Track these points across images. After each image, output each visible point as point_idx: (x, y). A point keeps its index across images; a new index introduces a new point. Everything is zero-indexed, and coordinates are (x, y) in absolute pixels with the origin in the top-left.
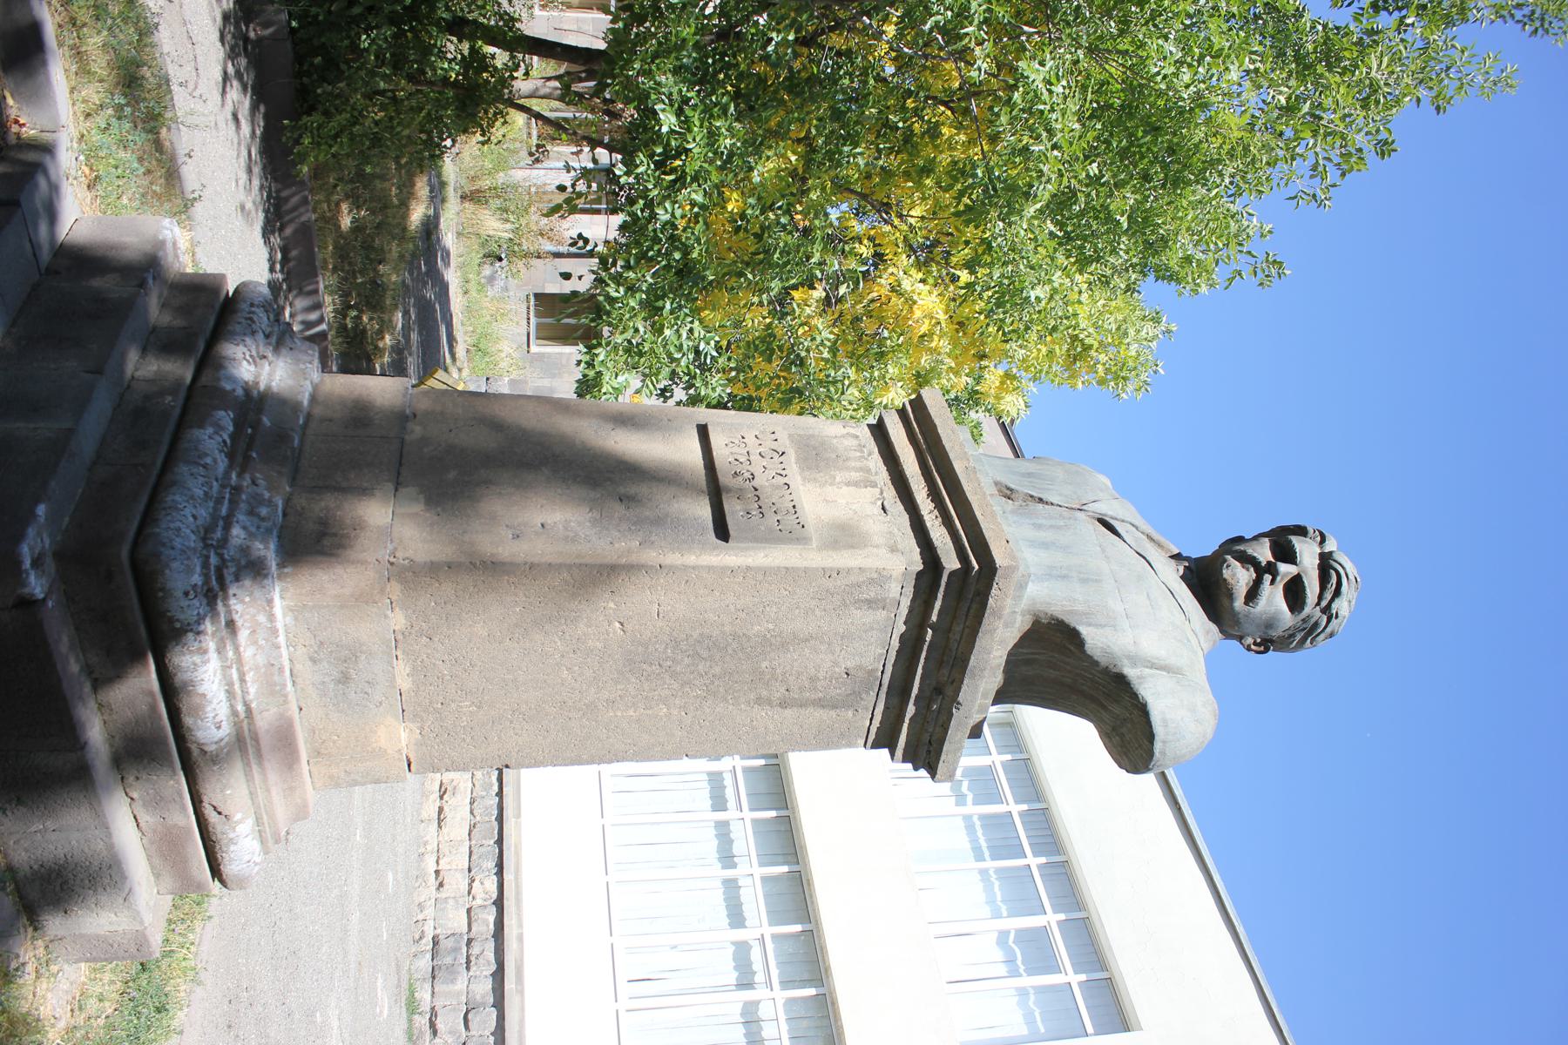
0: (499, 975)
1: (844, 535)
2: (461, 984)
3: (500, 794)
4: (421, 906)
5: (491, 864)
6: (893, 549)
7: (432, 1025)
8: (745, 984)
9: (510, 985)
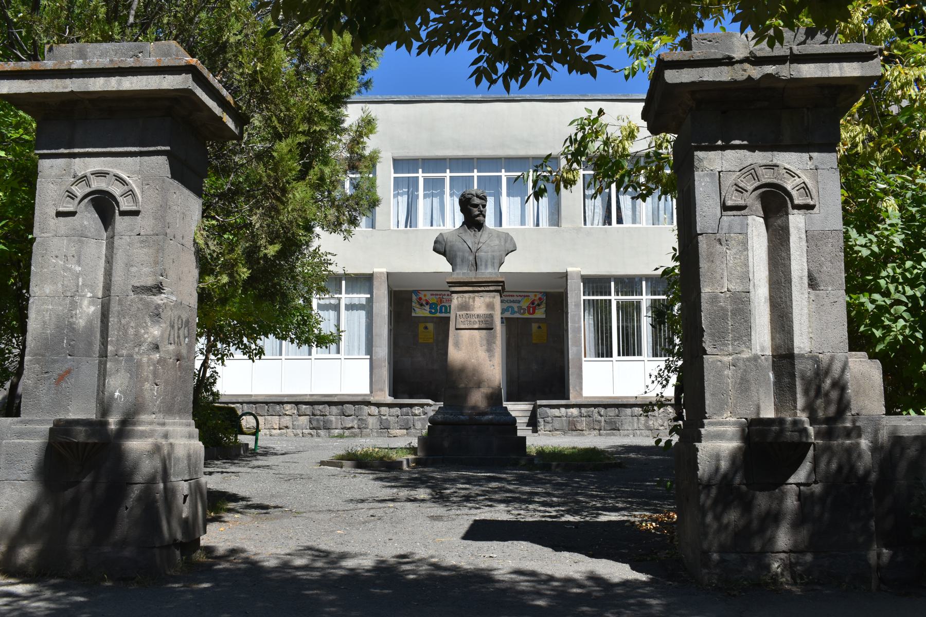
0: (330, 404)
1: (490, 306)
2: (333, 418)
5: (278, 407)
7: (349, 428)
8: (336, 308)
9: (336, 399)
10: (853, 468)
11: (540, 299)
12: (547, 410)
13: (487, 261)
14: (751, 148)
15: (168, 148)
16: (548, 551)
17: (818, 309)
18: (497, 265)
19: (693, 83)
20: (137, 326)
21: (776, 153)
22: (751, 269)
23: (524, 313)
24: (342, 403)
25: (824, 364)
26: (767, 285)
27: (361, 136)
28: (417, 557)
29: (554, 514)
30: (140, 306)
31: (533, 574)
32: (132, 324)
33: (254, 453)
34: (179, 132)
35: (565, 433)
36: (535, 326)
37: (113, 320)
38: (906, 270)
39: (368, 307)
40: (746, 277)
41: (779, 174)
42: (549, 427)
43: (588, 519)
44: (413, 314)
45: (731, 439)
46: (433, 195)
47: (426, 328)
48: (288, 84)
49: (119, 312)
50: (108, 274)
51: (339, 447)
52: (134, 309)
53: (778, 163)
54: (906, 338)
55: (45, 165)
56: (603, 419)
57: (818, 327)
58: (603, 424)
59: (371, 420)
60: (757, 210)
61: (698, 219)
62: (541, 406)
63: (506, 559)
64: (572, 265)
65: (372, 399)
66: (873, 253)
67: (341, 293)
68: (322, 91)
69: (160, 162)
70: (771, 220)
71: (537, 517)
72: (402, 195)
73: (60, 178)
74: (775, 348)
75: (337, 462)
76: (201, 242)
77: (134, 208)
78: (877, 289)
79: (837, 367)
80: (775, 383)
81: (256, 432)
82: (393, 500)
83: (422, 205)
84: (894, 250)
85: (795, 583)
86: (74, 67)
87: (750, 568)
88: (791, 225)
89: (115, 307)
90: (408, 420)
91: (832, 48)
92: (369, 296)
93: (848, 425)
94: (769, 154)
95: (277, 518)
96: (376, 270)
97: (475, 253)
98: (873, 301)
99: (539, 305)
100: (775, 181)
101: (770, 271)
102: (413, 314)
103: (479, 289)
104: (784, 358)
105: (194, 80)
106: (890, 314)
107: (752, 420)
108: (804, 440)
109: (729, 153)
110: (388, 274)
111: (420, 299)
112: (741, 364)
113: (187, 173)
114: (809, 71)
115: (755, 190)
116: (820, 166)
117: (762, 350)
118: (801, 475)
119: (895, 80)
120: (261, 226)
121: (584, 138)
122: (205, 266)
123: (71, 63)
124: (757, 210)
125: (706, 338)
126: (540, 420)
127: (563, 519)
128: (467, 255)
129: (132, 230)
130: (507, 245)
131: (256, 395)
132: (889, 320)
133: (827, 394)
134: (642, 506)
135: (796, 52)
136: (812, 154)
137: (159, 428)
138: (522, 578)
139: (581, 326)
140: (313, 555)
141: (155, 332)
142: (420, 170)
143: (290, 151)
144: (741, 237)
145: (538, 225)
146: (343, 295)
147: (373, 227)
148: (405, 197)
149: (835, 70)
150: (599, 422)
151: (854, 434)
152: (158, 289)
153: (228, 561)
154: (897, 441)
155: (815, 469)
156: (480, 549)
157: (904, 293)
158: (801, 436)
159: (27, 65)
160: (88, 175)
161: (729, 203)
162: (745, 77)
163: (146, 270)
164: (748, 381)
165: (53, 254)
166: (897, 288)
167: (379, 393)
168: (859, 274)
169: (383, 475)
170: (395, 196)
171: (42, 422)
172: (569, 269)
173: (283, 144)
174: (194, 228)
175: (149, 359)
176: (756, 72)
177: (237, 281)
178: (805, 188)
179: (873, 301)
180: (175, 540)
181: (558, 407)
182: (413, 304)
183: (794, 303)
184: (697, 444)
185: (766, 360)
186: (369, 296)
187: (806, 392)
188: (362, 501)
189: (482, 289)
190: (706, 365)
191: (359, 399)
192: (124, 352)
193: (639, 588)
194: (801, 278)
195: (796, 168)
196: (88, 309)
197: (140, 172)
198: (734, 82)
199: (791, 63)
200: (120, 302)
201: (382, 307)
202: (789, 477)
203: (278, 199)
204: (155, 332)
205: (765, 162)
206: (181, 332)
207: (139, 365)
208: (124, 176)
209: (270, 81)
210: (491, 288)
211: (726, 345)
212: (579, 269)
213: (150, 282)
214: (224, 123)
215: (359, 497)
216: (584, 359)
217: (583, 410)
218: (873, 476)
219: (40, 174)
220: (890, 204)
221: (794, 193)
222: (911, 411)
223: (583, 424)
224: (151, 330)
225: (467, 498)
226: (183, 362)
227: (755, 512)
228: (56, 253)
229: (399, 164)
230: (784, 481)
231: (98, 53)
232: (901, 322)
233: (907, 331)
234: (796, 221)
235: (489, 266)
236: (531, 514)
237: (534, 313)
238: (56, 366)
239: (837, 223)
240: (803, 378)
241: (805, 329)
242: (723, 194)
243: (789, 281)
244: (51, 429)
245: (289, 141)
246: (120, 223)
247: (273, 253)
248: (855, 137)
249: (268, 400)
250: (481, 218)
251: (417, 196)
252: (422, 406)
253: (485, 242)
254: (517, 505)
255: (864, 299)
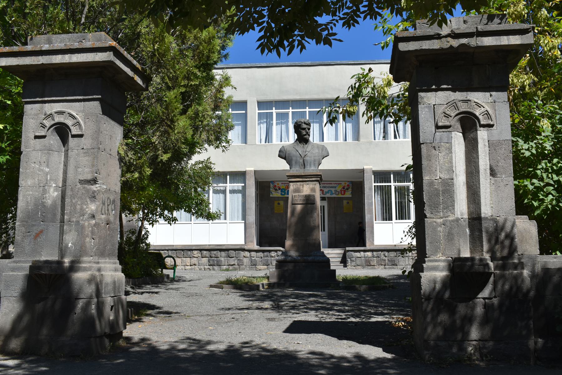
0: (221, 250)
1: (313, 190)
2: (222, 259)
3: (168, 250)
4: (200, 269)
5: (189, 252)
6: (315, 185)
7: (232, 265)
8: (224, 192)
9: (224, 248)
10: (519, 288)
11: (348, 185)
12: (353, 253)
13: (311, 162)
14: (454, 90)
15: (100, 97)
16: (334, 340)
17: (496, 188)
18: (317, 165)
19: (416, 50)
20: (82, 204)
21: (469, 93)
22: (454, 164)
23: (339, 194)
24: (228, 250)
25: (500, 224)
26: (465, 175)
27: (221, 87)
28: (254, 343)
29: (344, 317)
30: (84, 192)
31: (321, 354)
32: (79, 203)
33: (173, 280)
34: (107, 87)
35: (363, 267)
36: (345, 202)
37: (67, 200)
38: (553, 165)
39: (243, 192)
40: (451, 170)
41: (471, 106)
42: (353, 264)
43: (364, 320)
44: (271, 196)
45: (442, 271)
46: (282, 123)
47: (279, 204)
48: (173, 58)
49: (71, 195)
50: (65, 172)
51: (222, 276)
52: (80, 193)
53: (471, 99)
54: (553, 206)
55: (28, 107)
56: (387, 259)
57: (497, 200)
58: (387, 261)
59: (246, 261)
60: (458, 128)
61: (421, 134)
62: (349, 251)
63: (306, 345)
64: (367, 165)
65: (246, 247)
66: (532, 153)
67: (226, 183)
68: (195, 60)
69: (95, 105)
70: (467, 134)
71: (333, 319)
72: (263, 123)
73: (37, 116)
74: (470, 213)
75: (219, 286)
76: (122, 153)
77: (80, 133)
78: (535, 176)
79: (508, 225)
80: (470, 236)
81: (174, 267)
82: (247, 309)
83: (275, 129)
84: (546, 152)
85: (482, 360)
86: (44, 49)
87: (455, 350)
88: (479, 137)
89: (69, 193)
90: (268, 260)
91: (503, 27)
92: (243, 185)
93: (516, 261)
94: (465, 93)
95: (176, 319)
96: (247, 169)
97: (303, 158)
98: (533, 184)
99: (347, 189)
100: (469, 110)
101: (467, 166)
102: (271, 196)
103: (306, 180)
104: (475, 220)
105: (114, 55)
106: (544, 192)
107: (455, 258)
108: (487, 270)
109: (440, 93)
110: (255, 171)
111: (275, 186)
112: (448, 224)
113: (113, 111)
114: (488, 41)
115: (456, 116)
116: (497, 100)
117: (462, 215)
118: (486, 292)
119: (546, 46)
120: (159, 143)
121: (359, 86)
122: (127, 167)
123: (42, 47)
124: (458, 128)
125: (426, 207)
126: (349, 260)
127: (349, 320)
128: (299, 159)
129: (79, 146)
130: (323, 152)
131: (176, 246)
132: (543, 196)
133: (502, 243)
134: (398, 312)
135: (480, 30)
136: (491, 93)
137: (95, 265)
138: (315, 356)
139: (373, 201)
140: (189, 342)
141: (93, 207)
142: (274, 108)
143: (176, 97)
144: (447, 145)
145: (346, 140)
146: (228, 184)
147: (246, 143)
148: (265, 125)
149: (505, 41)
150: (385, 260)
151: (519, 267)
152: (94, 181)
153: (138, 346)
154: (546, 271)
155: (494, 289)
156: (293, 338)
157: (552, 179)
158: (484, 268)
159: (15, 49)
160: (53, 113)
161: (440, 124)
162: (448, 46)
163: (87, 170)
164: (452, 234)
165: (33, 161)
166: (548, 176)
167: (250, 243)
168: (522, 167)
169: (246, 293)
170: (259, 124)
171: (25, 262)
172: (365, 167)
173: (172, 93)
174: (118, 144)
175: (89, 224)
176: (455, 43)
177: (144, 176)
178: (487, 114)
179: (533, 184)
180: (105, 333)
181: (359, 251)
182: (271, 190)
183: (481, 186)
184: (421, 274)
185: (465, 221)
186: (243, 185)
187: (489, 241)
188: (229, 309)
189: (308, 179)
190: (426, 224)
191: (238, 247)
192: (74, 220)
193: (385, 363)
194: (486, 170)
195: (482, 102)
196: (53, 194)
197: (83, 111)
198: (442, 49)
199: (477, 37)
200: (72, 190)
201: (252, 191)
202: (478, 294)
203: (169, 126)
204: (93, 207)
205: (462, 98)
206: (110, 207)
207: (83, 227)
208: (74, 114)
209: (164, 55)
210: (313, 179)
211: (439, 212)
212: (371, 167)
213: (89, 177)
214: (135, 81)
215: (228, 307)
216: (375, 222)
217: (375, 253)
218: (532, 293)
219: (25, 113)
220: (545, 124)
221: (481, 117)
222: (558, 252)
223: (374, 262)
224: (90, 206)
225: (293, 308)
226: (111, 225)
227: (457, 316)
228: (35, 160)
229: (261, 104)
230: (475, 296)
231: (59, 40)
232: (550, 197)
233: (554, 202)
234: (482, 135)
235: (312, 166)
236: (329, 317)
237: (344, 194)
238: (35, 228)
239: (507, 135)
240: (487, 232)
241: (488, 202)
242: (436, 118)
243: (478, 172)
244: (30, 266)
245: (175, 91)
246: (72, 142)
247: (166, 159)
248: (524, 82)
249: (183, 248)
250: (307, 136)
251: (272, 124)
252: (276, 251)
253: (309, 151)
254: (322, 312)
255: (527, 182)
